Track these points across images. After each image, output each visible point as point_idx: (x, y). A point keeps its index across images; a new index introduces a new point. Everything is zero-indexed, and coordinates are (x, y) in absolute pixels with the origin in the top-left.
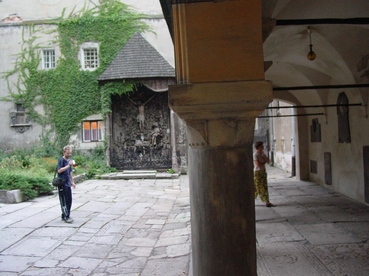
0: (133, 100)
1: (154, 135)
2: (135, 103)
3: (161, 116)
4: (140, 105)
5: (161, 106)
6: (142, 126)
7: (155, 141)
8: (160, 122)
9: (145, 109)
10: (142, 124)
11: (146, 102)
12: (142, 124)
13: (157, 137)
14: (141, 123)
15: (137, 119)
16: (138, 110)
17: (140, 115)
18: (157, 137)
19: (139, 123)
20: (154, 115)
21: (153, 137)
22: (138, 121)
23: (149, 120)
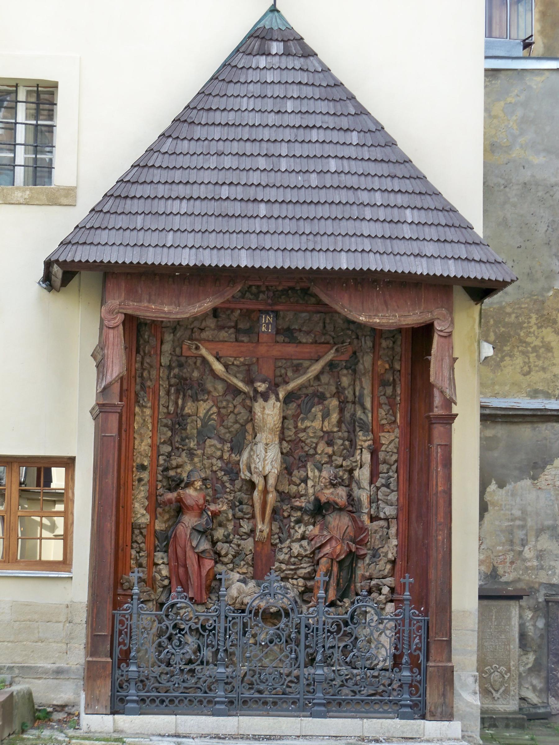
0: (226, 366)
1: (327, 549)
2: (241, 385)
3: (367, 457)
4: (265, 397)
5: (368, 405)
6: (264, 504)
7: (333, 584)
8: (360, 488)
9: (284, 418)
10: (265, 492)
11: (291, 386)
12: (265, 492)
13: (340, 563)
14: (260, 486)
15: (242, 466)
16: (251, 420)
17: (260, 448)
18: (340, 563)
19: (252, 485)
20: (330, 450)
21: (324, 564)
22: (245, 474)
23: (303, 473)
